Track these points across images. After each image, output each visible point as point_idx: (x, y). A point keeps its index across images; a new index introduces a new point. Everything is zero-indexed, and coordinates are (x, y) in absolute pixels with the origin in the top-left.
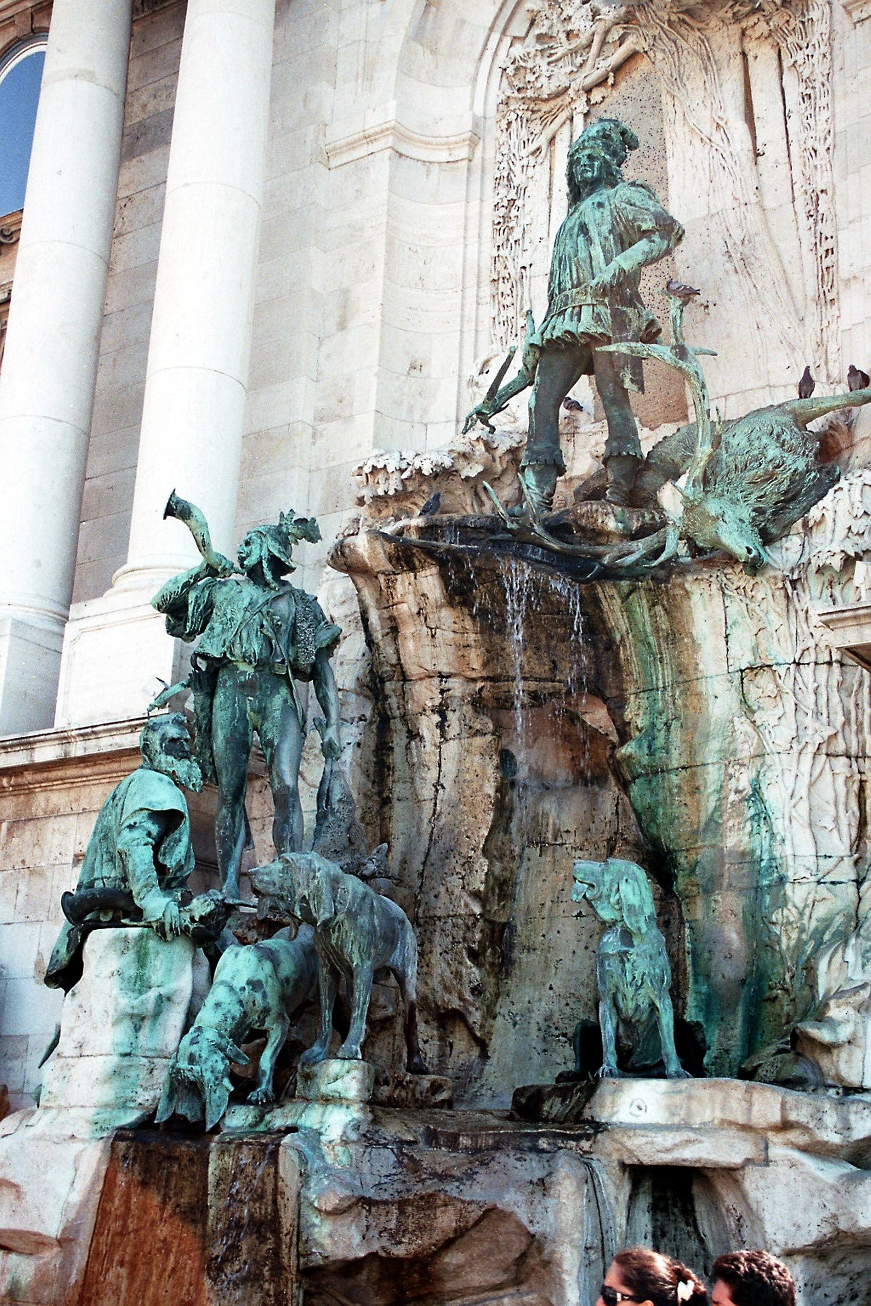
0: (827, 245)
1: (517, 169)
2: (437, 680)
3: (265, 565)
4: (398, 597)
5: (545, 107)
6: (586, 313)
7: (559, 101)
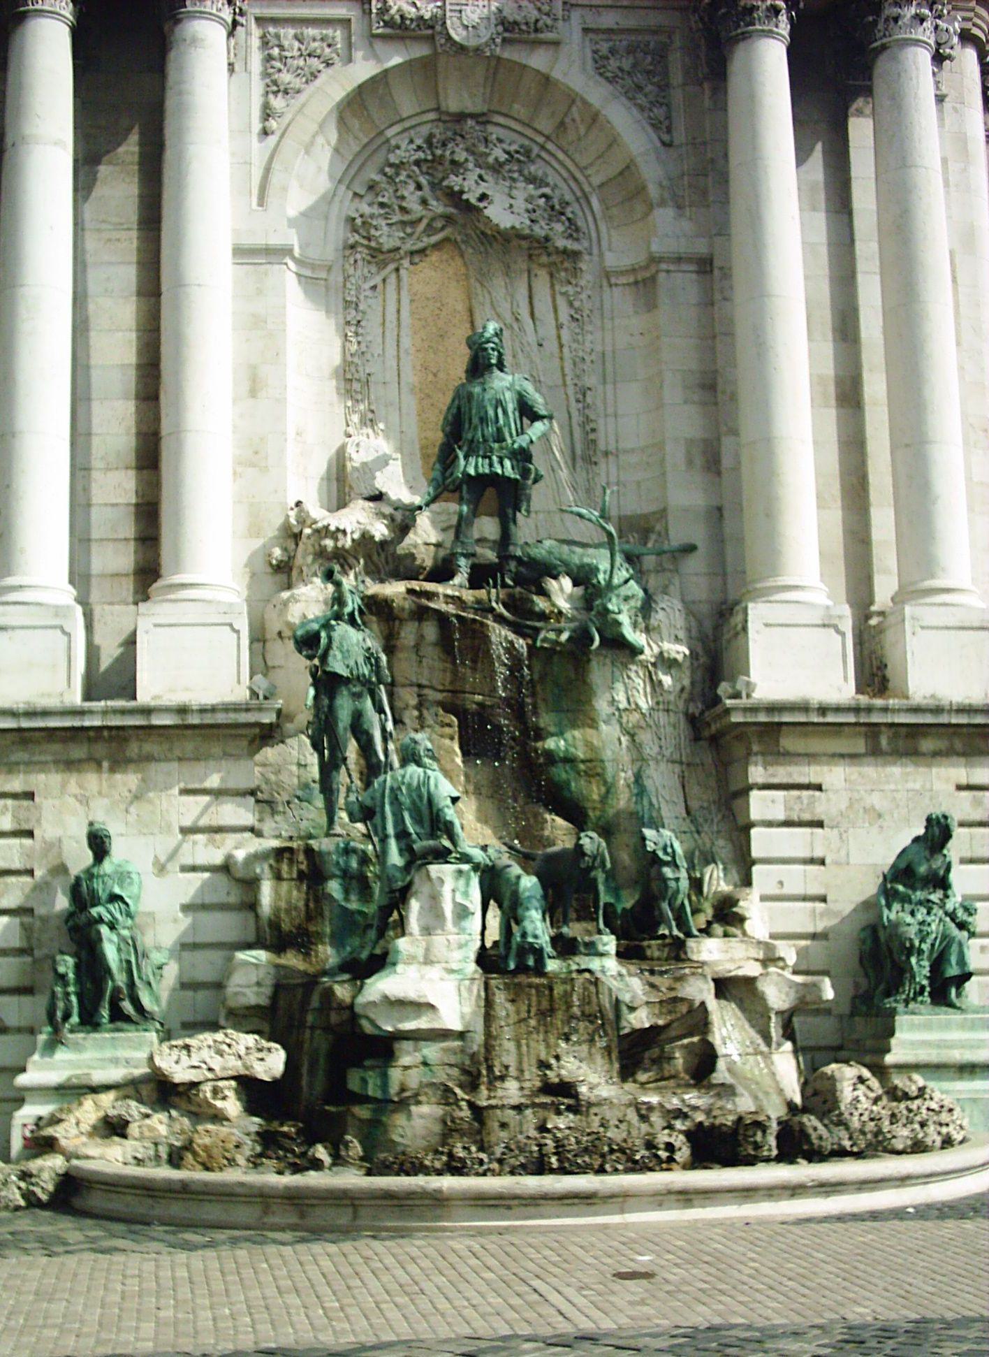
0: (592, 425)
1: (362, 297)
2: (416, 689)
3: (356, 613)
4: (403, 634)
5: (381, 257)
6: (507, 463)
7: (392, 255)
